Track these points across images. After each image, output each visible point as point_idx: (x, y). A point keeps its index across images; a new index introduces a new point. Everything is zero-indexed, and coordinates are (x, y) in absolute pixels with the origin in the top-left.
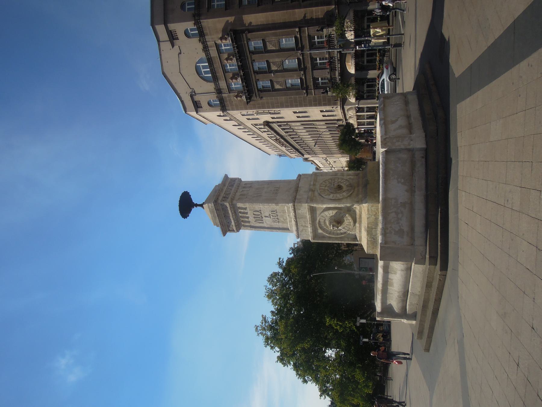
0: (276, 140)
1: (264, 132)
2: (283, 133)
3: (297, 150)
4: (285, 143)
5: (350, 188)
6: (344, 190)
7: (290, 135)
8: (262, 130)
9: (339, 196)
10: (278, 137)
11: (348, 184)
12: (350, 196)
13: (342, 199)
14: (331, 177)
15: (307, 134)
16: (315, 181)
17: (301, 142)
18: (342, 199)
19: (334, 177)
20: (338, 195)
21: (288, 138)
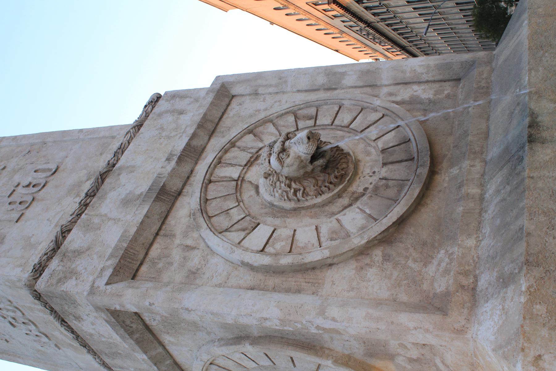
0: (361, 30)
1: (335, 16)
2: (368, 16)
3: (403, 48)
4: (377, 35)
5: (399, 171)
6: (357, 187)
7: (383, 20)
8: (330, 14)
9: (310, 235)
10: (362, 25)
11: (390, 139)
12: (386, 238)
13: (328, 264)
14: (300, 98)
15: (416, 14)
16: (209, 126)
17: (406, 32)
18: (328, 264)
19: (322, 95)
20: (305, 234)
21: (382, 26)
